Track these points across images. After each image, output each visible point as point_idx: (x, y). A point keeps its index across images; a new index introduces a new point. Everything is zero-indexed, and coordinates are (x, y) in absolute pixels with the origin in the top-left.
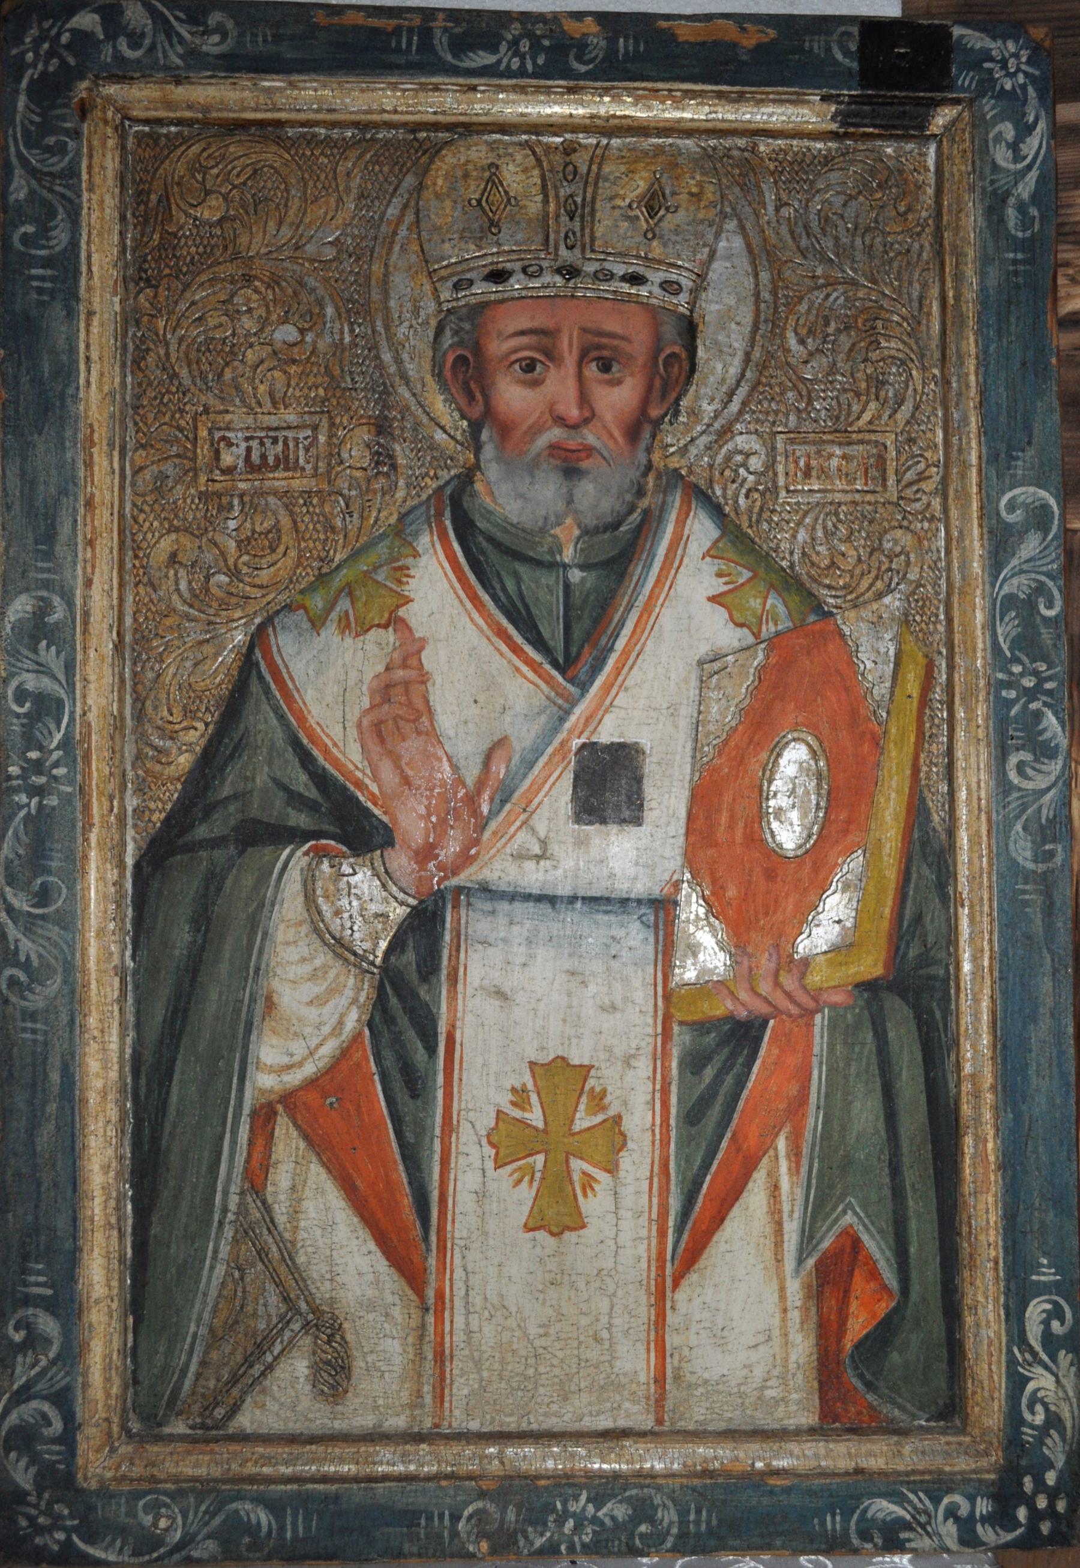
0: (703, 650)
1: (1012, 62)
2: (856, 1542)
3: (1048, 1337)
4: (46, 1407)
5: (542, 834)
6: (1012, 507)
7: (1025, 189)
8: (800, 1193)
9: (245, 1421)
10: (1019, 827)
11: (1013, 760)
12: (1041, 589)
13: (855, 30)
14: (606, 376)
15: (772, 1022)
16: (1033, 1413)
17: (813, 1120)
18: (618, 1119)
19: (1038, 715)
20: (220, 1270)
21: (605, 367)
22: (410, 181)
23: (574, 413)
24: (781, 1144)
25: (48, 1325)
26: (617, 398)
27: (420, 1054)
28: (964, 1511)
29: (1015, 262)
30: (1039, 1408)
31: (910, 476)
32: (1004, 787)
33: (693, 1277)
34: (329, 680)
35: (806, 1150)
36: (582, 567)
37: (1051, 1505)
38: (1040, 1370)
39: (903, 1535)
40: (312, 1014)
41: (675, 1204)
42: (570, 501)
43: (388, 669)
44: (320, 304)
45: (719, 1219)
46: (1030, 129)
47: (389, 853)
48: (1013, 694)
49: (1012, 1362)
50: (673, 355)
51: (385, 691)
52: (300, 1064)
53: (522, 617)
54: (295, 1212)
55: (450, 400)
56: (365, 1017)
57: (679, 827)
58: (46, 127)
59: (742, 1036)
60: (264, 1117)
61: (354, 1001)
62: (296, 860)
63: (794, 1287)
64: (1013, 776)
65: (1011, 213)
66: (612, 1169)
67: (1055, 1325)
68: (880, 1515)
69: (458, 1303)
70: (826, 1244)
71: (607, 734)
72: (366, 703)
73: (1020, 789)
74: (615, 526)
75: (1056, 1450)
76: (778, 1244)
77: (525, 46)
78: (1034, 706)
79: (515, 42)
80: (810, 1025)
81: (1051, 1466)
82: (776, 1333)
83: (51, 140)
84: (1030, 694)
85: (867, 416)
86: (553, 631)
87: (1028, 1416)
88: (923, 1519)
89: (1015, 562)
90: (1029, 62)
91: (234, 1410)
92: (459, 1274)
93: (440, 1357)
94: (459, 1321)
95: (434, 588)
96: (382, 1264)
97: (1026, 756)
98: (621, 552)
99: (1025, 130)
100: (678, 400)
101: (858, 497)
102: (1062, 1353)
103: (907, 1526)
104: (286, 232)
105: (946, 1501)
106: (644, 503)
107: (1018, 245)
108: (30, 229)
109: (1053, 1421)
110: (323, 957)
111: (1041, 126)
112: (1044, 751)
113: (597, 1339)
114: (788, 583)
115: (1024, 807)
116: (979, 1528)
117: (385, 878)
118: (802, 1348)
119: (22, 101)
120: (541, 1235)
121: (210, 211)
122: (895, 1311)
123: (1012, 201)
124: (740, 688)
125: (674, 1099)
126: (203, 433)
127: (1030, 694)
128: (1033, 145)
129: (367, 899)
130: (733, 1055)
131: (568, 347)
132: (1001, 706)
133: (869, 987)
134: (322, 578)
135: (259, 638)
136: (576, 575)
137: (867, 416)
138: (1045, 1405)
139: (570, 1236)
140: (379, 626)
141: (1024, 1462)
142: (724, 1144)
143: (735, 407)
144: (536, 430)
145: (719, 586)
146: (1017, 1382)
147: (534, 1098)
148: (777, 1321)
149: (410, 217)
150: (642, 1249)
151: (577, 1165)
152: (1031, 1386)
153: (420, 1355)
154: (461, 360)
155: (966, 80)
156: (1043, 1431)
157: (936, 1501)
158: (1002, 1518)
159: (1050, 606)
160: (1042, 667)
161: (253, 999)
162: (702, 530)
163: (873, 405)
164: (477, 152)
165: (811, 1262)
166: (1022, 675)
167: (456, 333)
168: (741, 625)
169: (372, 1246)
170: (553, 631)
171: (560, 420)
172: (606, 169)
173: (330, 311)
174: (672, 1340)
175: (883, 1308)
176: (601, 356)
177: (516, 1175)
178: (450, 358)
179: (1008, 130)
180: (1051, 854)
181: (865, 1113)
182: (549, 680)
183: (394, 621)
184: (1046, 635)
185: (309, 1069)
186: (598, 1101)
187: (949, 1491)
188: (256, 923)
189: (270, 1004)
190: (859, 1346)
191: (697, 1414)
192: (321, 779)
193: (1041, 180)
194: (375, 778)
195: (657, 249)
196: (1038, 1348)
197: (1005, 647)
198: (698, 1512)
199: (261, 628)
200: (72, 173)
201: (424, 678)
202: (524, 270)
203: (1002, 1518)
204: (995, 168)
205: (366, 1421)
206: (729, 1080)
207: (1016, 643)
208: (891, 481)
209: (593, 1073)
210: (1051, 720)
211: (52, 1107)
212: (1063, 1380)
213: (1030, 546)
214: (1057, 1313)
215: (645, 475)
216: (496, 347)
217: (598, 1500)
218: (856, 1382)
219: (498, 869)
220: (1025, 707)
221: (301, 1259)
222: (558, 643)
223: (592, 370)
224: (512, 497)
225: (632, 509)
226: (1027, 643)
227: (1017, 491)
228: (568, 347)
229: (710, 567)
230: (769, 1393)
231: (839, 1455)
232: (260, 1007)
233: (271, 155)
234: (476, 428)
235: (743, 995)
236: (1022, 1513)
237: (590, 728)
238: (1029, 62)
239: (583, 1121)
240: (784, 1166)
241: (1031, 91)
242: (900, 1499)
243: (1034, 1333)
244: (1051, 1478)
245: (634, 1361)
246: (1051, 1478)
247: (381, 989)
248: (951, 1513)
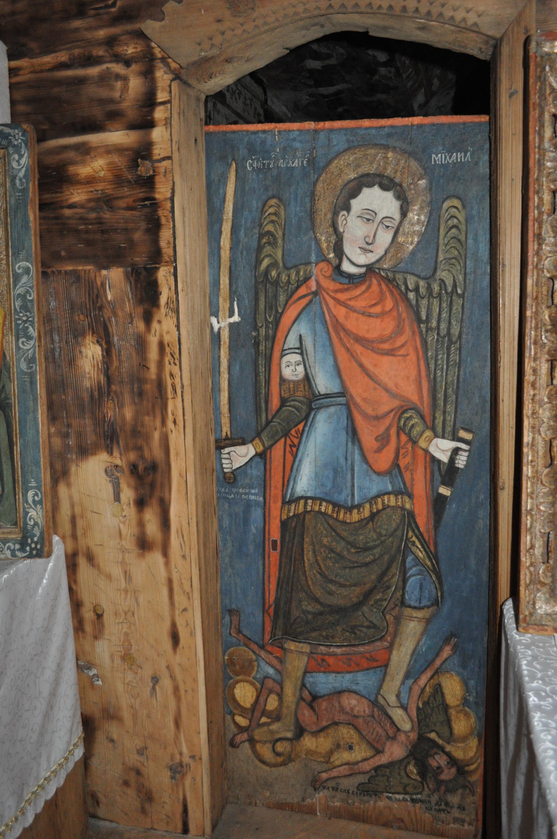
1: (17, 136)
3: (34, 501)
6: (19, 268)
7: (21, 174)
10: (23, 360)
11: (21, 341)
12: (28, 292)
19: (27, 328)
28: (12, 548)
29: (19, 196)
30: (32, 520)
37: (36, 546)
38: (32, 510)
48: (20, 322)
65: (18, 182)
67: (36, 498)
75: (37, 532)
78: (26, 325)
81: (36, 536)
84: (25, 322)
87: (29, 522)
89: (20, 284)
90: (22, 136)
97: (24, 339)
99: (21, 156)
107: (20, 191)
109: (36, 524)
111: (26, 155)
112: (29, 338)
115: (24, 354)
116: (17, 552)
123: (18, 178)
127: (25, 322)
128: (23, 161)
141: (28, 534)
152: (30, 514)
156: (33, 526)
157: (5, 545)
158: (22, 549)
159: (30, 296)
160: (28, 314)
180: (32, 367)
187: (8, 542)
193: (26, 171)
196: (31, 504)
197: (18, 308)
203: (22, 549)
204: (13, 168)
207: (21, 308)
213: (25, 279)
214: (36, 494)
227: (21, 263)
238: (22, 136)
241: (23, 145)
243: (30, 500)
244: (36, 539)
246: (36, 539)
248: (9, 548)
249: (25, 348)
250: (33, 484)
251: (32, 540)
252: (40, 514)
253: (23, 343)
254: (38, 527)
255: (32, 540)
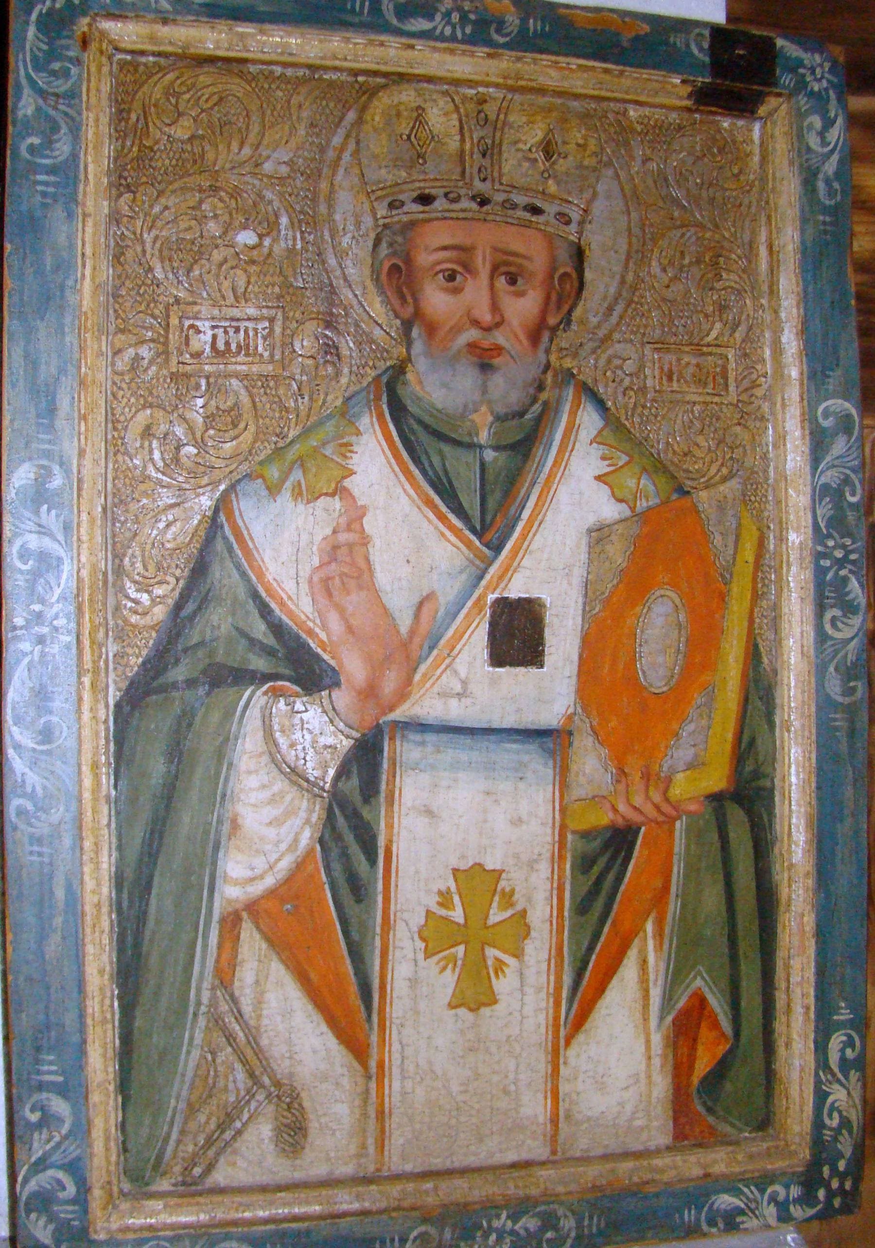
0: (591, 520)
2: (705, 1227)
3: (843, 1060)
4: (61, 1175)
5: (463, 675)
6: (826, 414)
7: (831, 167)
8: (662, 966)
9: (220, 1176)
10: (831, 669)
11: (828, 615)
12: (846, 481)
13: (707, 33)
14: (512, 288)
15: (643, 829)
16: (831, 1118)
17: (673, 907)
18: (524, 913)
20: (196, 1053)
21: (512, 280)
22: (351, 116)
23: (487, 318)
24: (649, 927)
25: (60, 1106)
26: (523, 307)
27: (361, 864)
28: (781, 1198)
29: (824, 223)
30: (835, 1115)
31: (746, 383)
32: (821, 637)
33: (581, 1037)
34: (284, 542)
35: (667, 930)
36: (496, 448)
38: (836, 1086)
39: (738, 1219)
40: (271, 833)
41: (567, 980)
42: (484, 390)
43: (335, 532)
44: (277, 216)
45: (600, 988)
46: (833, 122)
47: (335, 694)
48: (827, 563)
49: (818, 1082)
50: (565, 274)
51: (333, 551)
52: (261, 877)
53: (444, 488)
54: (259, 1002)
55: (387, 302)
56: (317, 835)
57: (571, 669)
58: (53, 55)
59: (619, 841)
60: (231, 923)
61: (307, 821)
62: (256, 698)
63: (657, 1039)
64: (828, 628)
65: (821, 185)
66: (518, 954)
68: (723, 1206)
69: (396, 1071)
70: (681, 1004)
71: (515, 591)
72: (316, 562)
73: (832, 638)
74: (521, 414)
76: (646, 1006)
77: (455, 17)
78: (843, 573)
79: (448, 14)
80: (671, 832)
81: (842, 1156)
82: (643, 1076)
83: (56, 66)
84: (840, 563)
85: (714, 334)
86: (471, 502)
87: (827, 1121)
88: (753, 1206)
89: (828, 458)
90: (830, 72)
91: (210, 1168)
92: (396, 1047)
93: (381, 1115)
94: (396, 1085)
95: (373, 464)
96: (332, 1042)
97: (837, 612)
98: (526, 438)
99: (829, 123)
100: (570, 312)
101: (708, 399)
102: (852, 1072)
103: (742, 1212)
104: (247, 151)
105: (769, 1191)
106: (544, 396)
107: (825, 210)
108: (36, 140)
109: (845, 1123)
110: (280, 784)
112: (849, 608)
113: (506, 1092)
114: (658, 467)
115: (836, 652)
116: (792, 1208)
117: (333, 713)
118: (661, 1086)
119: (31, 31)
120: (462, 1012)
121: (181, 132)
122: (731, 1051)
123: (821, 176)
124: (617, 553)
125: (567, 895)
126: (174, 321)
127: (840, 563)
129: (316, 732)
130: (613, 858)
131: (482, 264)
132: (820, 572)
133: (716, 798)
134: (278, 452)
135: (223, 505)
136: (489, 455)
137: (714, 334)
138: (840, 1112)
139: (485, 1011)
140: (326, 494)
141: (824, 1155)
142: (606, 929)
143: (614, 319)
144: (457, 330)
145: (603, 468)
146: (821, 1096)
147: (456, 899)
148: (643, 1067)
149: (352, 146)
150: (542, 1018)
151: (491, 953)
153: (365, 1115)
154: (395, 268)
155: (786, 80)
156: (838, 1131)
157: (762, 1191)
158: (808, 1199)
159: (853, 494)
161: (220, 822)
162: (589, 420)
163: (718, 325)
164: (407, 96)
165: (669, 1018)
166: (834, 548)
167: (391, 245)
168: (620, 501)
169: (324, 1028)
170: (471, 502)
171: (476, 323)
172: (511, 118)
173: (284, 220)
174: (564, 1088)
175: (722, 1049)
176: (507, 269)
177: (442, 964)
178: (386, 266)
179: (816, 121)
180: (853, 690)
181: (712, 899)
182: (469, 544)
183: (340, 491)
184: (851, 516)
185: (270, 881)
186: (508, 898)
187: (772, 1183)
188: (222, 754)
189: (235, 825)
190: (704, 1081)
191: (582, 1145)
192: (277, 629)
193: (841, 162)
194: (324, 627)
195: (552, 187)
196: (836, 1070)
198: (591, 1218)
199: (225, 495)
200: (72, 95)
201: (365, 541)
202: (446, 195)
203: (808, 1199)
205: (320, 1170)
206: (611, 877)
207: (830, 523)
208: (732, 388)
209: (504, 875)
210: (854, 584)
211: (58, 921)
212: (853, 1093)
213: (839, 446)
214: (850, 1043)
215: (545, 372)
216: (424, 259)
217: (515, 1217)
218: (700, 1108)
219: (427, 706)
220: (837, 573)
221: (264, 1042)
222: (475, 512)
223: (501, 282)
224: (439, 387)
225: (535, 400)
226: (837, 522)
228: (482, 264)
229: (596, 451)
230: (637, 1123)
231: (690, 1165)
232: (226, 828)
233: (236, 87)
234: (407, 325)
235: (622, 807)
236: (821, 1194)
237: (502, 585)
239: (496, 916)
240: (651, 944)
242: (738, 1193)
244: (842, 1165)
245: (534, 1107)
246: (842, 1165)
247: (330, 811)
248: (773, 1199)
249: (838, 635)
250: (844, 1015)
251: (834, 1170)
252: (857, 1094)
253: (833, 620)
254: (850, 1132)
255: (834, 1170)
